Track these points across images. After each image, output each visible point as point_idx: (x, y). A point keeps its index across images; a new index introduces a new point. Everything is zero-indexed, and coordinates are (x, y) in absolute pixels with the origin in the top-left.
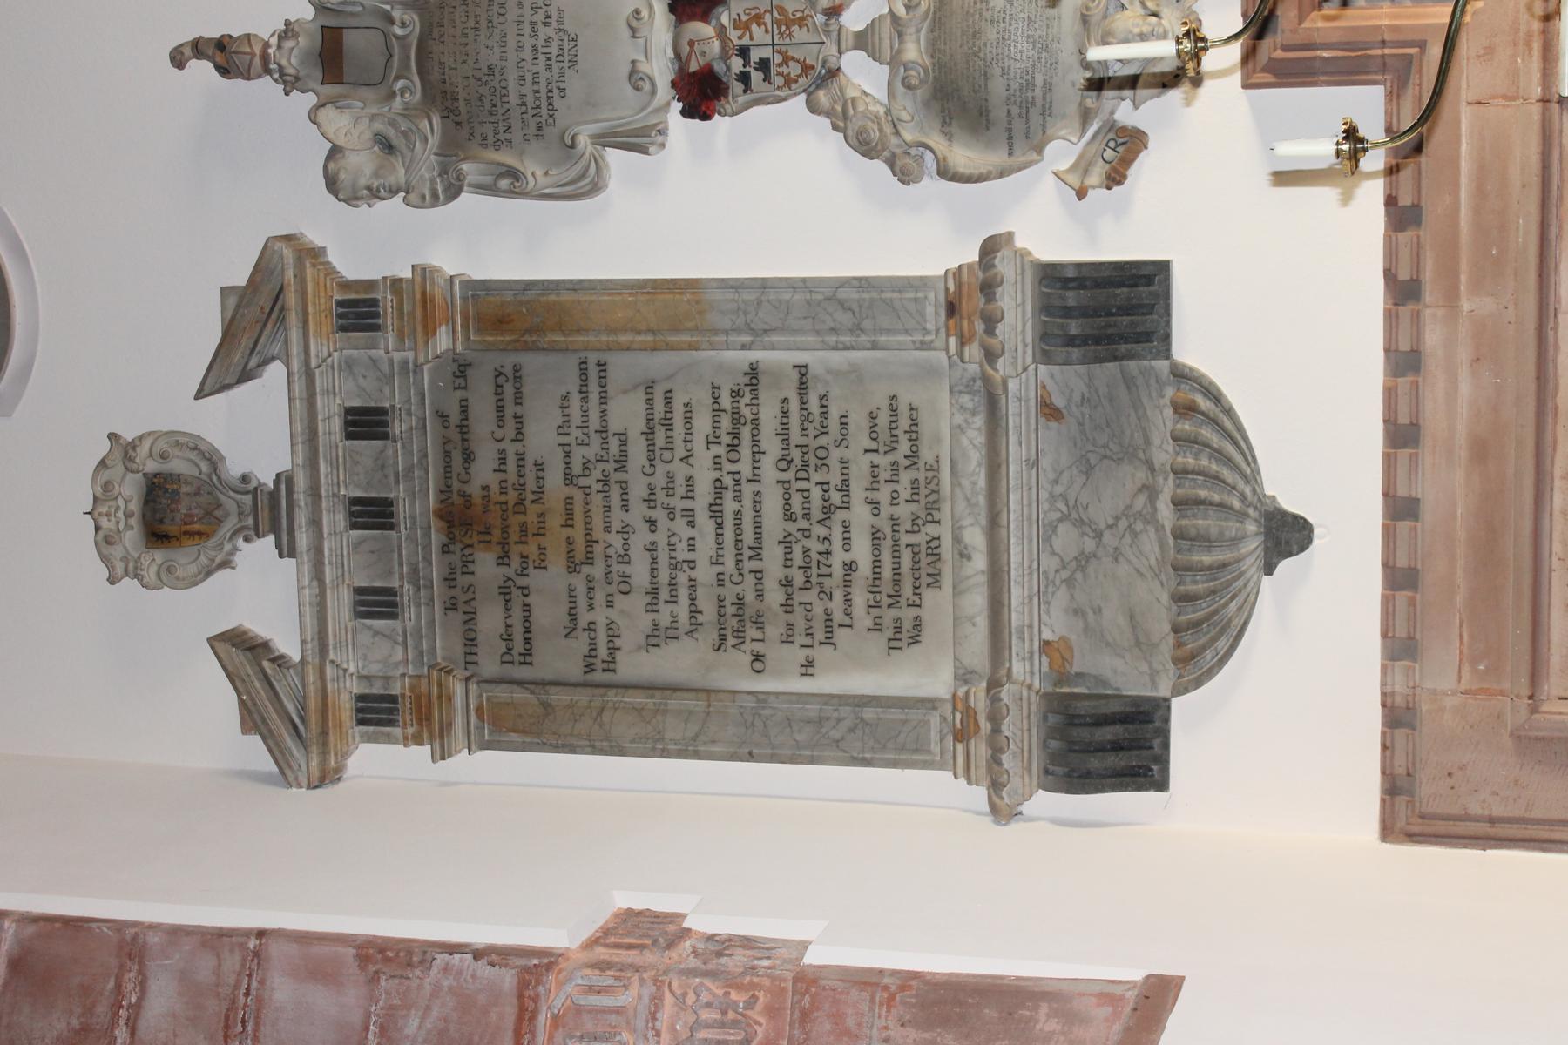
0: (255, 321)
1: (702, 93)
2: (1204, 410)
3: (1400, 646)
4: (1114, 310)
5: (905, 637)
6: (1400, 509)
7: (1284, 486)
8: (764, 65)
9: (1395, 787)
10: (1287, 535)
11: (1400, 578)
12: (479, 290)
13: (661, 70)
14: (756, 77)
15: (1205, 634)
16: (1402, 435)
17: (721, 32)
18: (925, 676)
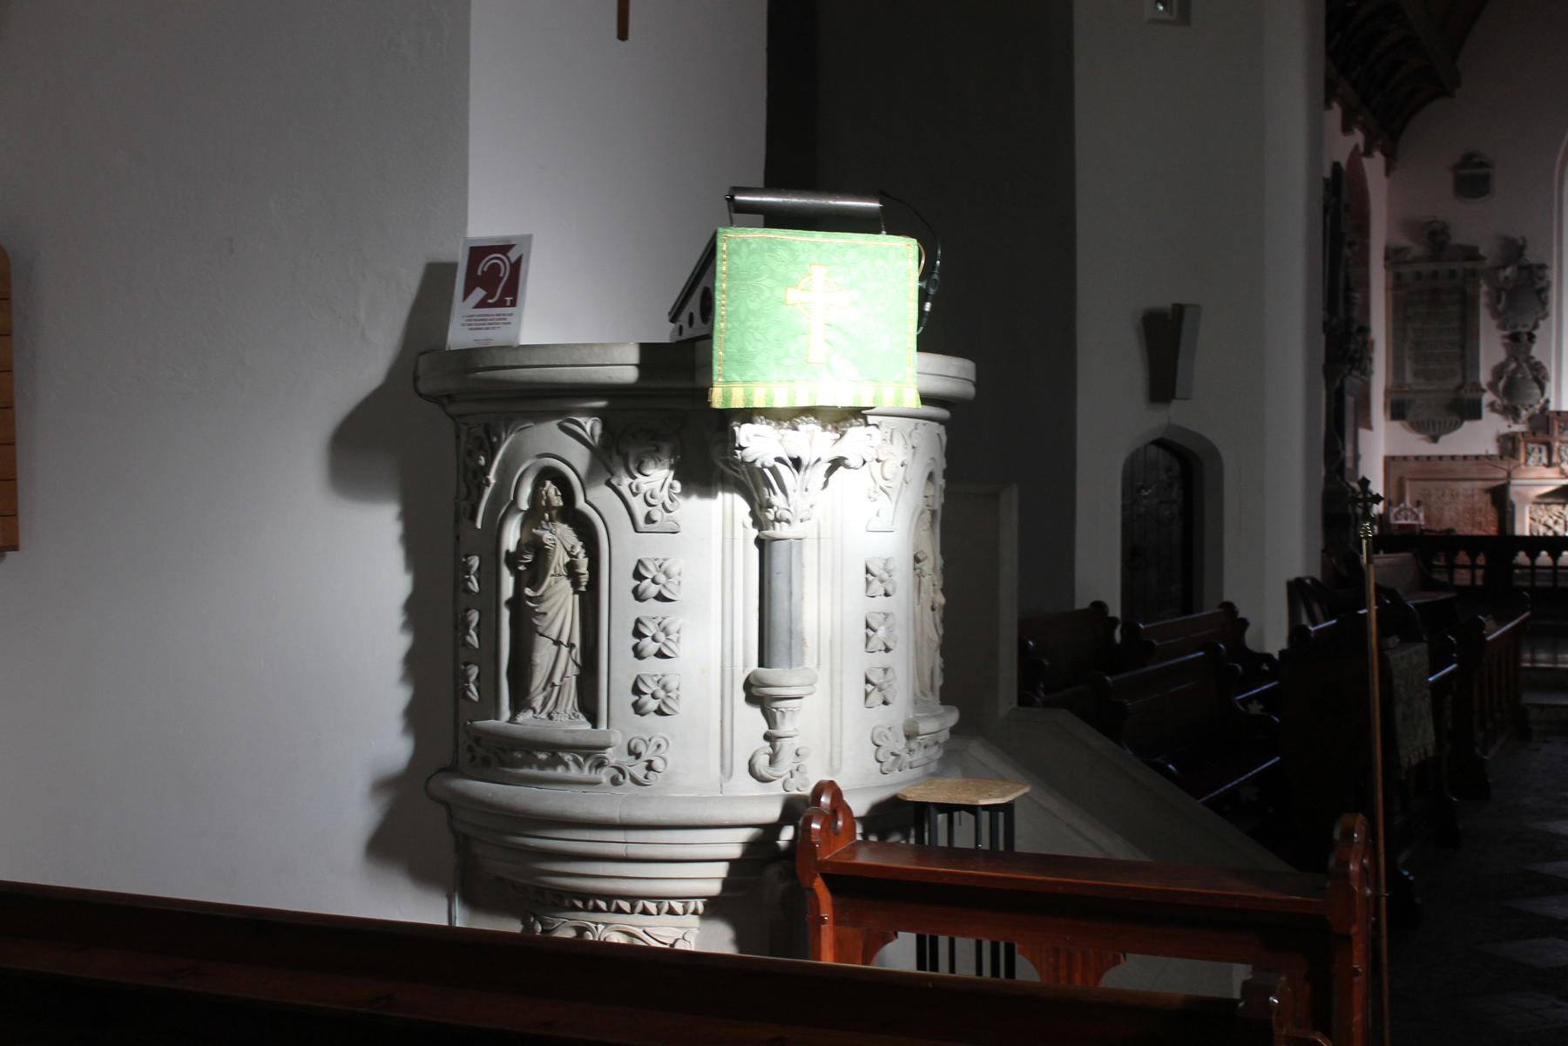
0: (1471, 254)
1: (1515, 338)
2: (1456, 426)
3: (1417, 458)
4: (1474, 413)
5: (1416, 374)
6: (1440, 458)
7: (1443, 439)
9: (1393, 458)
10: (1435, 439)
11: (1429, 458)
12: (1478, 296)
13: (1520, 329)
15: (1418, 427)
16: (1453, 457)
18: (1409, 378)
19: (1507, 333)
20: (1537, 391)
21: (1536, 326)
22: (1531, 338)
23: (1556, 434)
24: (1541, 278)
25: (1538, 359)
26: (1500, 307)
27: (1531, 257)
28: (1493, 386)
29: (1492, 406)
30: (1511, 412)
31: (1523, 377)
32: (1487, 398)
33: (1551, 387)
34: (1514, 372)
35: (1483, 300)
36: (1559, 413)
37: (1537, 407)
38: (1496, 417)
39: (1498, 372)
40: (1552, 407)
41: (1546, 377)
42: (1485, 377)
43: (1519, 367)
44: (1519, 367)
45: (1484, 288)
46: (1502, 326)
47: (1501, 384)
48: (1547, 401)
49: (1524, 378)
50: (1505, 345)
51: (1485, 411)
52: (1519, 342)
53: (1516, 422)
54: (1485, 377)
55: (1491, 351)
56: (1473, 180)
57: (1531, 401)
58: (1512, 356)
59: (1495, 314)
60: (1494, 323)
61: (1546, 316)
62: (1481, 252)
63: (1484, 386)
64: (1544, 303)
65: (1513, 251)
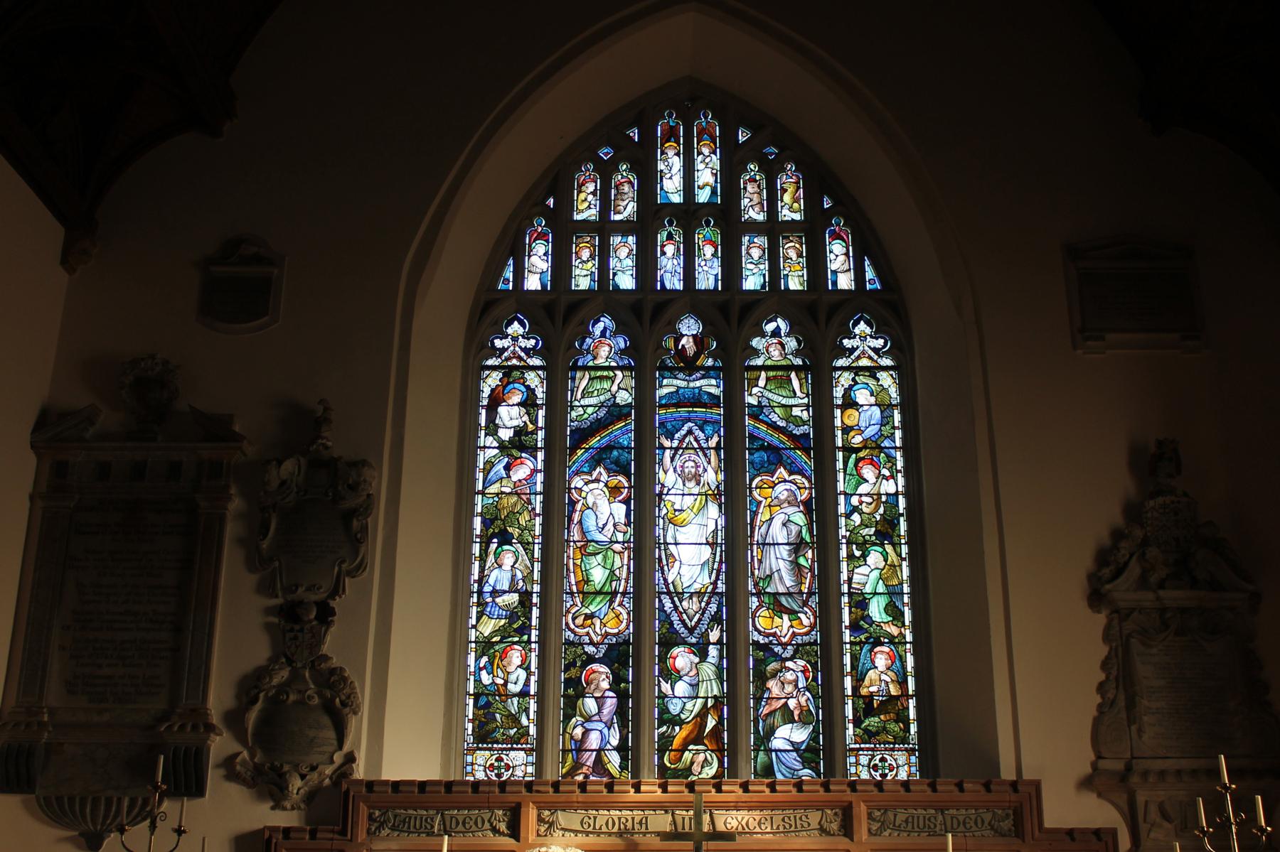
0: (217, 429)
1: (290, 613)
8: (296, 638)
12: (222, 520)
14: (292, 634)
17: (310, 621)
19: (279, 601)
20: (331, 734)
21: (337, 590)
22: (326, 614)
23: (362, 836)
24: (354, 488)
25: (335, 662)
26: (265, 545)
27: (336, 443)
28: (234, 720)
29: (228, 764)
30: (268, 784)
31: (308, 699)
32: (220, 745)
33: (359, 727)
34: (283, 688)
35: (231, 530)
36: (370, 785)
37: (329, 771)
38: (235, 792)
39: (249, 687)
40: (360, 771)
41: (350, 704)
42: (218, 699)
43: (296, 676)
44: (296, 676)
45: (236, 504)
46: (266, 588)
47: (253, 716)
48: (350, 758)
49: (301, 703)
50: (268, 627)
51: (213, 777)
52: (300, 622)
53: (277, 806)
54: (218, 699)
55: (238, 641)
56: (237, 289)
57: (315, 759)
58: (282, 654)
59: (255, 560)
60: (253, 579)
61: (361, 567)
62: (237, 428)
63: (215, 719)
64: (357, 541)
65: (302, 426)
